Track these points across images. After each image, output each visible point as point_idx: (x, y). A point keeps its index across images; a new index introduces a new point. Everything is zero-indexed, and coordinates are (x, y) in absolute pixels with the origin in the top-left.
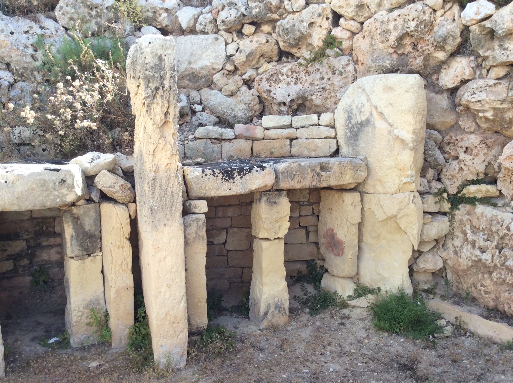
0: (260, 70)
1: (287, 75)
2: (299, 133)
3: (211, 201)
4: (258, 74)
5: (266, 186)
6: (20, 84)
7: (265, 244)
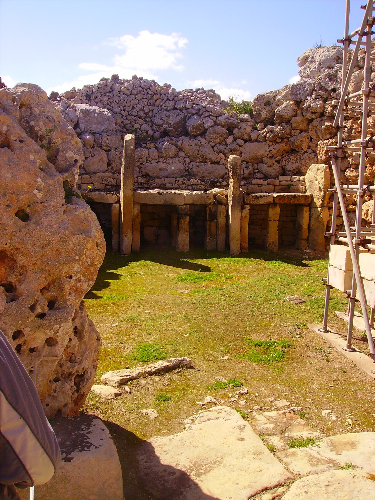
0: (283, 156)
1: (293, 160)
2: (293, 183)
3: (251, 205)
4: (282, 158)
5: (270, 202)
6: (192, 163)
7: (270, 223)
